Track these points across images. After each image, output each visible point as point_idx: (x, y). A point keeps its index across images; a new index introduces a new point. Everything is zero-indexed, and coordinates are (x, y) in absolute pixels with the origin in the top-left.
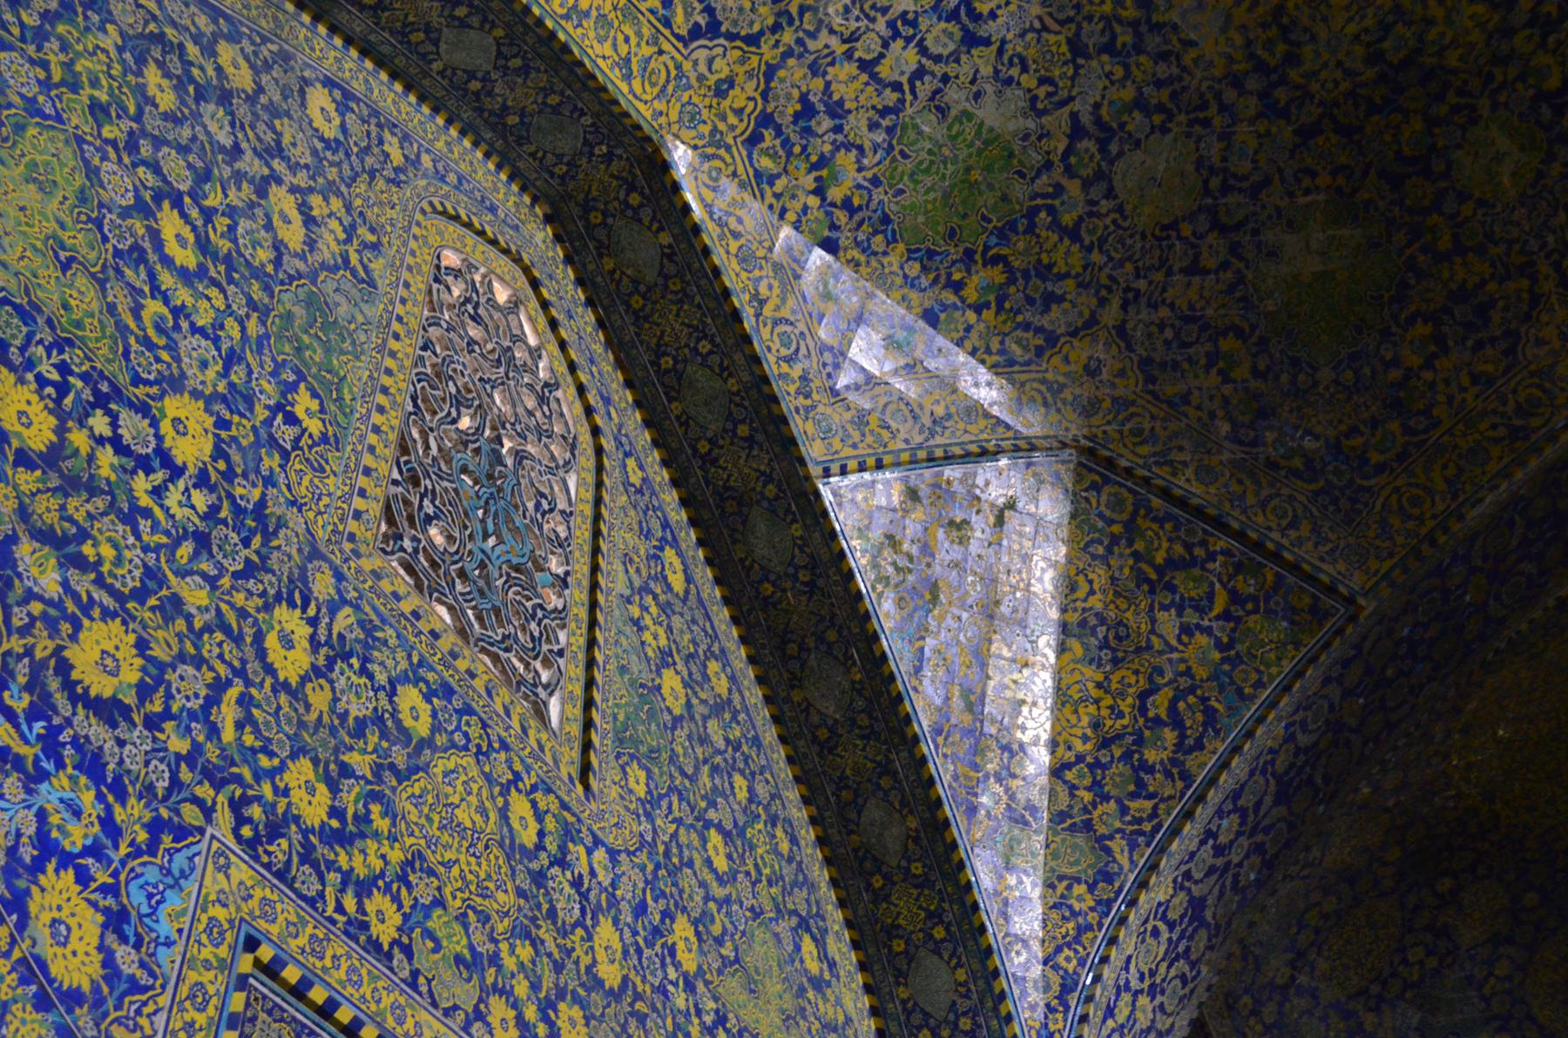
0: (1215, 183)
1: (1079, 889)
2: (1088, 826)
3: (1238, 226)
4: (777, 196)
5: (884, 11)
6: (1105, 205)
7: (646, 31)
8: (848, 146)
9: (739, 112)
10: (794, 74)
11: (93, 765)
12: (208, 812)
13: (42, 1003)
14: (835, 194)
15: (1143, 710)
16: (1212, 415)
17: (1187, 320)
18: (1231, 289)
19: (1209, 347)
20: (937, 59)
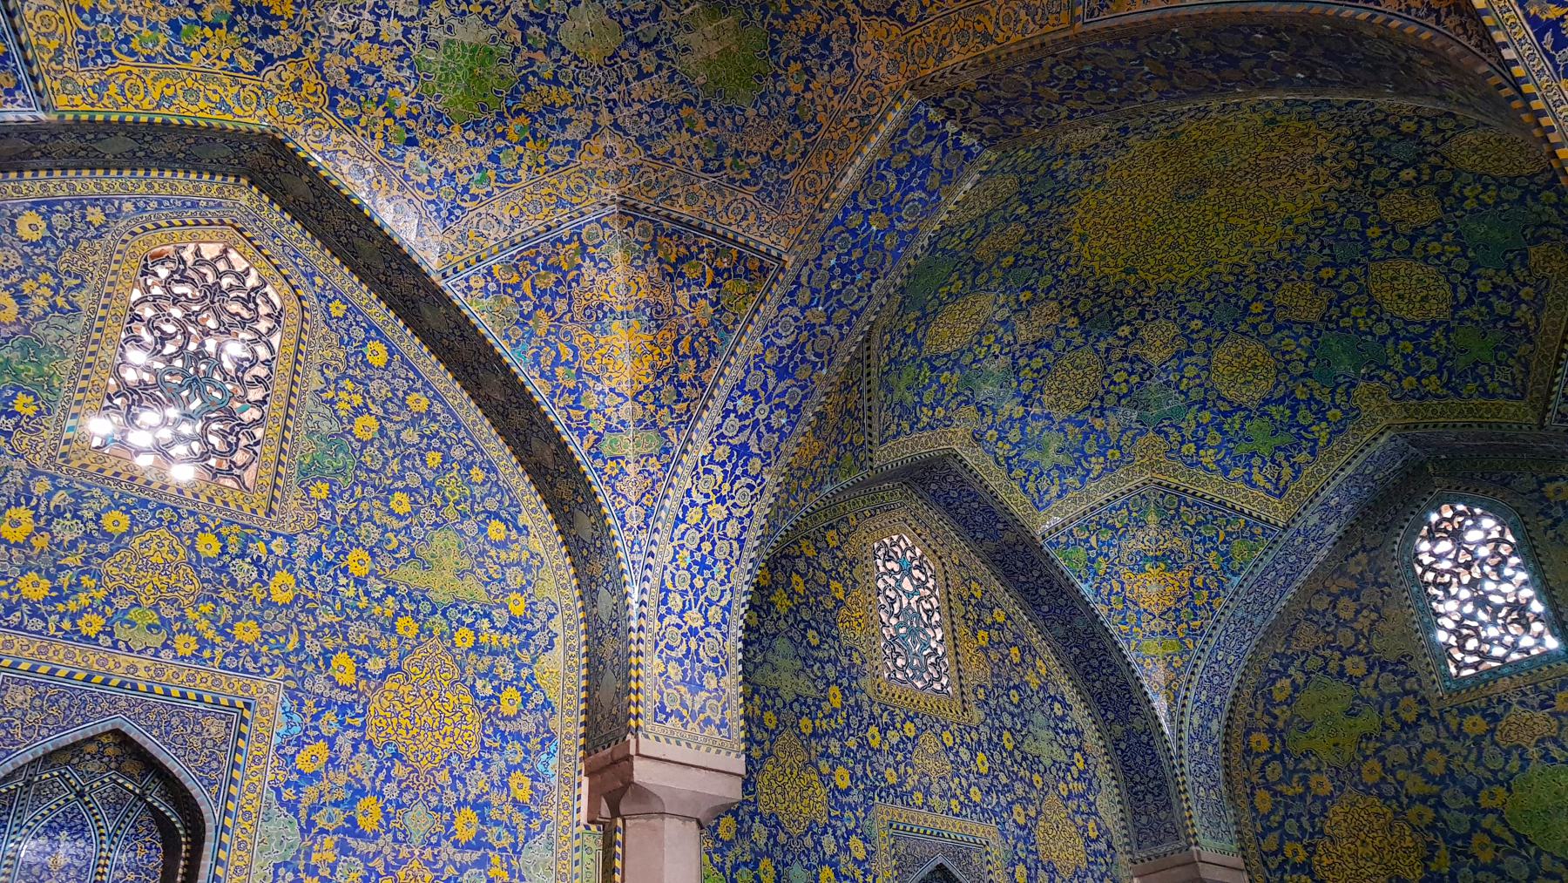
0: (626, 21)
2: (654, 424)
3: (656, 41)
4: (364, 128)
5: (363, 6)
6: (565, 59)
7: (226, 81)
8: (392, 85)
10: (334, 62)
15: (676, 351)
16: (691, 159)
17: (653, 106)
18: (671, 79)
19: (674, 117)
20: (412, 19)
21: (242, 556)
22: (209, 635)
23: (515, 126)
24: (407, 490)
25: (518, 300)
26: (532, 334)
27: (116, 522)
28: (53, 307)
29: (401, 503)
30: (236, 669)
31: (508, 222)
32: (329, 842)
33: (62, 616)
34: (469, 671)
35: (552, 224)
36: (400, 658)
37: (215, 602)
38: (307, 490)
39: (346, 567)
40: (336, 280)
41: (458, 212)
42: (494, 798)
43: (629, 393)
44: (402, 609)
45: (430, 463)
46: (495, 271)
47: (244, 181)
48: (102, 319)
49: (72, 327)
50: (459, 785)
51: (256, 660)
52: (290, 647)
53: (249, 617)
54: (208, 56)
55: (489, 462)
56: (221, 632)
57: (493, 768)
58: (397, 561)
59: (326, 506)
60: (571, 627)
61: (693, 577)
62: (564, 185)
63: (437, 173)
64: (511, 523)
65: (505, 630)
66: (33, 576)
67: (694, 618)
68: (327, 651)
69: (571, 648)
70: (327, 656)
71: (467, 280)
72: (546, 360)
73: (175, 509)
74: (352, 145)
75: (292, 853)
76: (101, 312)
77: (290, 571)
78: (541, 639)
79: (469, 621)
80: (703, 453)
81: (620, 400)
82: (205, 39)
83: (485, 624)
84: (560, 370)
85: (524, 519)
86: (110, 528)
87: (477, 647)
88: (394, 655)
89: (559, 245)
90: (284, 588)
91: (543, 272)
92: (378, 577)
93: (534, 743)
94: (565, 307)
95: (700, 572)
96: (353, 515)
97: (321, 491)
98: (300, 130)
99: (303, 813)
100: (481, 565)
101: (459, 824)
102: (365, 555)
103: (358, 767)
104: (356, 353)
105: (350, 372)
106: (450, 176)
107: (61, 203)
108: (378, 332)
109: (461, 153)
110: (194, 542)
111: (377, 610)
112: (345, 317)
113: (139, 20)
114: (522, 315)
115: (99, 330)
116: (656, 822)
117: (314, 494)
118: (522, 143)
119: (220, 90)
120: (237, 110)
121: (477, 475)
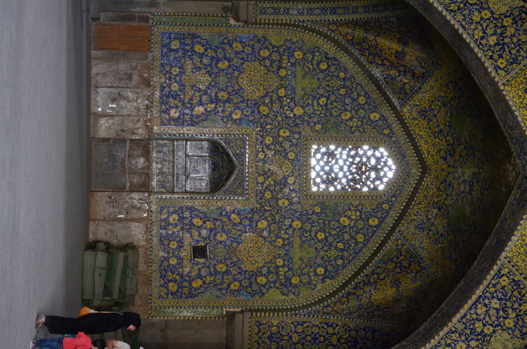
1: (347, 311)
4: (439, 194)
7: (436, 150)
8: (452, 196)
10: (451, 176)
11: (253, 112)
12: (257, 127)
13: (229, 114)
14: (446, 202)
21: (290, 190)
22: (265, 185)
23: (451, 237)
24: (326, 238)
25: (397, 256)
26: (386, 264)
27: (291, 156)
28: (351, 127)
29: (321, 236)
30: (256, 193)
31: (422, 246)
32: (212, 226)
33: (263, 148)
34: (269, 265)
35: (424, 259)
36: (269, 241)
37: (275, 185)
38: (316, 205)
39: (294, 221)
40: (396, 205)
41: (422, 230)
42: (230, 277)
43: (371, 300)
44: (285, 240)
45: (339, 245)
46: (405, 247)
47: (421, 170)
48: (352, 140)
49: (347, 133)
50: (233, 265)
51: (260, 199)
52: (266, 208)
53: (272, 195)
54: (439, 143)
55: (346, 266)
56: (266, 188)
57: (239, 276)
58: (300, 237)
59: (313, 212)
60: (292, 302)
61: (310, 335)
62: (438, 259)
63: (433, 220)
65: (285, 276)
66: (271, 139)
67: (295, 338)
68: (267, 218)
69: (284, 303)
70: (266, 219)
71: (400, 239)
72: (378, 270)
73: (300, 169)
74: (433, 192)
75: (209, 216)
76: (354, 139)
77: (289, 204)
78: (285, 290)
79: (286, 263)
80: (351, 325)
81: (369, 297)
82: (442, 140)
83: (286, 269)
84: (376, 276)
85: (328, 281)
86: (289, 154)
87: (278, 267)
88: (269, 239)
89: (418, 264)
90: (283, 203)
91: (408, 261)
92: (293, 231)
93: (249, 290)
94: (398, 271)
95: (312, 338)
97: (317, 210)
98: (432, 176)
99: (219, 218)
100: (306, 266)
101: (221, 265)
102: (299, 226)
103: (234, 232)
104: (371, 215)
105: (363, 214)
106: (433, 224)
107: (386, 122)
108: (382, 222)
109: (440, 224)
110: (291, 176)
111: (283, 232)
112: (384, 210)
113: (438, 121)
115: (348, 140)
116: (225, 328)
117: (316, 208)
118: (448, 242)
119: (432, 150)
121: (340, 262)
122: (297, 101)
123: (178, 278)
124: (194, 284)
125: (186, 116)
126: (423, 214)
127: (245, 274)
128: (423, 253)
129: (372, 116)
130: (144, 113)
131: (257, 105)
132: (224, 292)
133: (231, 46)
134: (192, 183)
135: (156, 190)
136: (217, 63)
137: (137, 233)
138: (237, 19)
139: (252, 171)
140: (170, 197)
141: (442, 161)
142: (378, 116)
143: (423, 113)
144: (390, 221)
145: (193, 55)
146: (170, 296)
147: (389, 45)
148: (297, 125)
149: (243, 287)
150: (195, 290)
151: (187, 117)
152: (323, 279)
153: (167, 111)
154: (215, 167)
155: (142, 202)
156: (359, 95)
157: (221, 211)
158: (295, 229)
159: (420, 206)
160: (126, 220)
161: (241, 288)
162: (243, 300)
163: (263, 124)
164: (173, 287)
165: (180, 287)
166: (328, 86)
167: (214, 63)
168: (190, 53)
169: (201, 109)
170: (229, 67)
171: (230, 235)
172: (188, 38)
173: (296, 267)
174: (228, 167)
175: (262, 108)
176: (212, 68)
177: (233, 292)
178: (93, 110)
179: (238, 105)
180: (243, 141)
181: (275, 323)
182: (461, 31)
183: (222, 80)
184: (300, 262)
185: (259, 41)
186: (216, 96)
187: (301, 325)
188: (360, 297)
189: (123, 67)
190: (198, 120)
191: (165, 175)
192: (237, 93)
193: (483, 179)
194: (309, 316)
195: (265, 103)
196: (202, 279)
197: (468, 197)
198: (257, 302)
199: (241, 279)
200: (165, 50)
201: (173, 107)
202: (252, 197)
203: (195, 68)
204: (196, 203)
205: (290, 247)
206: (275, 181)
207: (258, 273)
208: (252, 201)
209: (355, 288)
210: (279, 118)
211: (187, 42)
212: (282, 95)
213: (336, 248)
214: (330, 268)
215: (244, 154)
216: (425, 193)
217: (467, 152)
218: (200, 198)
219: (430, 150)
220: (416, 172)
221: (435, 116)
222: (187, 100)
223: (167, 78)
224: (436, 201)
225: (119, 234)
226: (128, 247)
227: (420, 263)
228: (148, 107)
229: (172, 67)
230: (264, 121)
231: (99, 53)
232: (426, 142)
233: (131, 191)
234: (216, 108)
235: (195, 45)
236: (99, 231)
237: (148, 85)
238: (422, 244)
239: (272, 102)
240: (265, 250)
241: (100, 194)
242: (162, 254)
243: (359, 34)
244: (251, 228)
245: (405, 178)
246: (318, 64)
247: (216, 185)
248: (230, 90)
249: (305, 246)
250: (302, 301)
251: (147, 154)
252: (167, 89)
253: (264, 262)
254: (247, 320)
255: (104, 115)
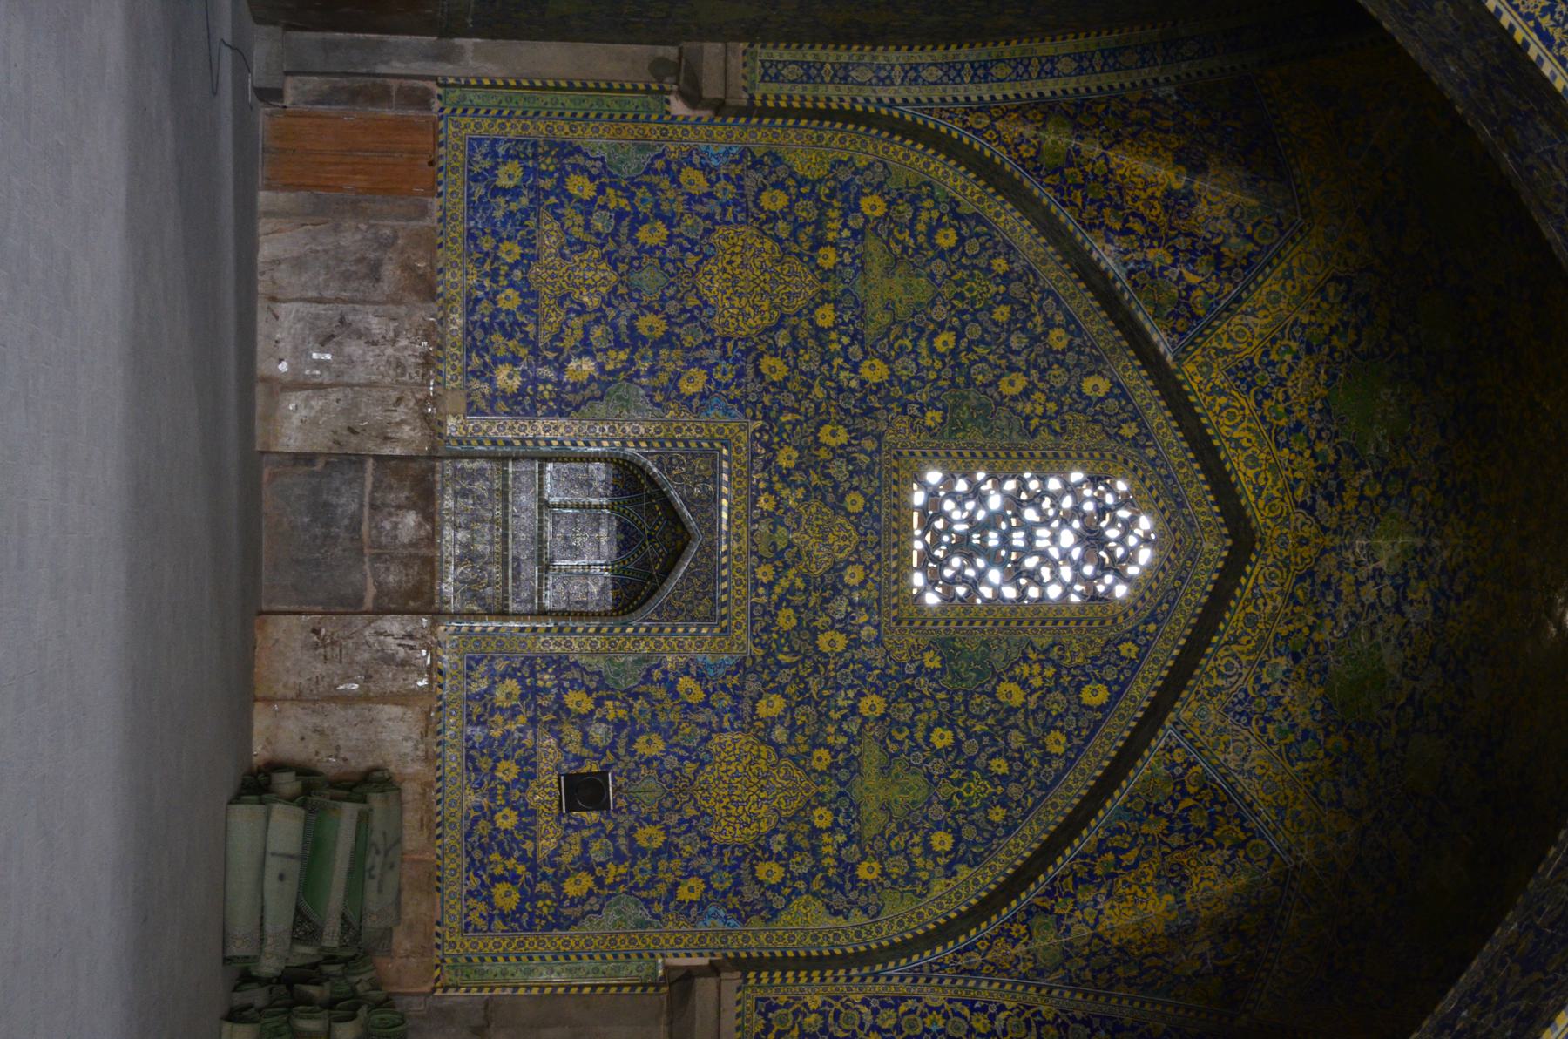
1: (1030, 965)
4: (1293, 613)
7: (1280, 485)
8: (1334, 618)
9: (1303, 559)
10: (1331, 560)
11: (740, 374)
12: (754, 418)
14: (1316, 637)
20: (1382, 605)
21: (851, 603)
22: (777, 590)
23: (1338, 740)
24: (958, 742)
25: (1171, 798)
26: (1141, 821)
27: (855, 502)
28: (1028, 418)
29: (942, 738)
31: (1247, 766)
32: (622, 713)
33: (769, 481)
34: (792, 826)
35: (1256, 807)
36: (790, 757)
37: (806, 590)
38: (929, 649)
39: (864, 695)
41: (1244, 720)
42: (676, 863)
43: (1100, 929)
44: (838, 752)
45: (994, 763)
46: (1195, 769)
47: (1229, 542)
48: (1032, 455)
49: (1015, 436)
50: (683, 828)
51: (764, 630)
52: (780, 657)
53: (799, 619)
54: (1290, 462)
55: (1016, 826)
56: (782, 598)
57: (704, 860)
58: (883, 742)
59: (918, 669)
60: (858, 934)
62: (1299, 808)
63: (1276, 690)
64: (955, 859)
65: (839, 860)
66: (795, 454)
68: (784, 688)
69: (837, 936)
70: (780, 689)
71: (1179, 746)
72: (1117, 841)
73: (879, 543)
74: (1274, 608)
75: (611, 685)
76: (1037, 454)
77: (848, 646)
78: (838, 900)
79: (841, 821)
80: (1044, 1009)
81: (1091, 922)
82: (1301, 454)
83: (841, 838)
84: (1110, 856)
85: (964, 871)
86: (848, 499)
87: (816, 832)
88: (792, 750)
89: (1237, 821)
90: (832, 643)
91: (1206, 813)
92: (862, 725)
93: (734, 901)
94: (1176, 844)
96: (916, 694)
97: (932, 661)
99: (643, 689)
100: (900, 827)
101: (650, 830)
102: (879, 711)
103: (687, 730)
104: (1087, 675)
105: (1064, 672)
106: (1277, 702)
107: (1129, 401)
108: (1120, 693)
109: (1300, 702)
110: (853, 563)
111: (831, 729)
112: (1123, 659)
113: (1287, 398)
114: (1157, 806)
115: (1020, 455)
116: (664, 1019)
117: (928, 656)
118: (1327, 754)
120: (1261, 503)
121: (998, 814)
122: (869, 341)
123: (521, 869)
124: (571, 889)
125: (541, 388)
126: (1245, 672)
127: (720, 854)
128: (1251, 789)
129: (1088, 385)
130: (418, 379)
131: (752, 353)
132: (658, 909)
133: (675, 181)
134: (560, 587)
135: (452, 608)
136: (633, 229)
137: (395, 736)
138: (693, 98)
139: (740, 548)
140: (497, 629)
141: (1300, 517)
142: (1104, 386)
143: (1243, 375)
144: (1142, 690)
145: (562, 205)
146: (498, 923)
147: (1147, 171)
148: (869, 412)
149: (716, 892)
150: (573, 904)
151: (546, 390)
152: (948, 867)
153: (485, 373)
154: (627, 539)
155: (411, 643)
156: (1049, 324)
157: (649, 669)
158: (865, 720)
159: (1235, 648)
160: (365, 698)
161: (710, 895)
162: (716, 932)
163: (770, 408)
164: (506, 897)
165: (529, 896)
166: (960, 296)
167: (624, 229)
168: (553, 200)
169: (588, 366)
170: (670, 240)
171: (676, 739)
172: (546, 154)
173: (872, 830)
174: (668, 537)
175: (767, 362)
176: (618, 244)
177: (685, 909)
178: (263, 367)
179: (697, 354)
180: (713, 461)
181: (814, 1001)
182: (1533, 52)
183: (649, 278)
184: (882, 818)
185: (757, 164)
186: (632, 328)
187: (890, 1006)
188: (1067, 922)
189: (352, 238)
190: (579, 398)
191: (481, 562)
192: (693, 318)
193: (1443, 569)
194: (915, 980)
195: (777, 348)
196: (591, 871)
197: (1393, 621)
198: (756, 938)
199: (709, 869)
200: (479, 190)
201: (503, 361)
202: (739, 625)
203: (570, 244)
204: (575, 645)
205: (853, 773)
206: (806, 580)
207: (760, 850)
208: (739, 637)
209: (1049, 894)
210: (818, 392)
211: (543, 167)
212: (826, 323)
213: (987, 773)
214: (968, 833)
215: (714, 499)
216: (1250, 609)
217: (1384, 487)
218: (586, 630)
219: (1262, 482)
220: (1214, 547)
221: (1280, 382)
222: (544, 340)
223: (486, 275)
224: (1284, 633)
225: (340, 741)
226: (368, 783)
227: (1243, 820)
228: (427, 361)
229: (501, 240)
230: (774, 401)
231: (282, 199)
232: (1253, 461)
233: (381, 611)
234: (631, 361)
235: (568, 174)
236: (280, 733)
237: (430, 294)
238: (1249, 761)
239: (795, 344)
240: (778, 780)
241: (284, 621)
242: (472, 798)
243: (1057, 139)
244: (738, 718)
245: (1184, 567)
246: (931, 232)
247: (634, 590)
248: (672, 307)
249: (897, 769)
250: (889, 932)
251: (425, 500)
252: (485, 307)
253: (774, 817)
254: (730, 996)
255: (297, 384)
